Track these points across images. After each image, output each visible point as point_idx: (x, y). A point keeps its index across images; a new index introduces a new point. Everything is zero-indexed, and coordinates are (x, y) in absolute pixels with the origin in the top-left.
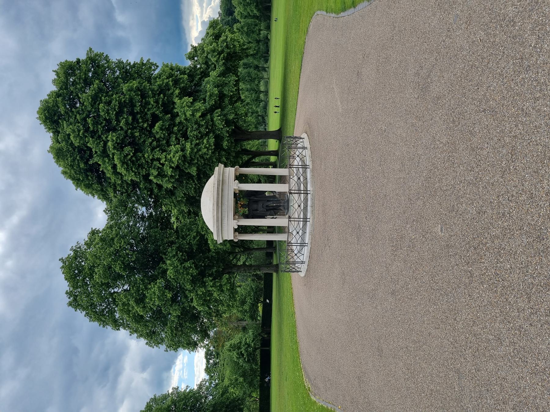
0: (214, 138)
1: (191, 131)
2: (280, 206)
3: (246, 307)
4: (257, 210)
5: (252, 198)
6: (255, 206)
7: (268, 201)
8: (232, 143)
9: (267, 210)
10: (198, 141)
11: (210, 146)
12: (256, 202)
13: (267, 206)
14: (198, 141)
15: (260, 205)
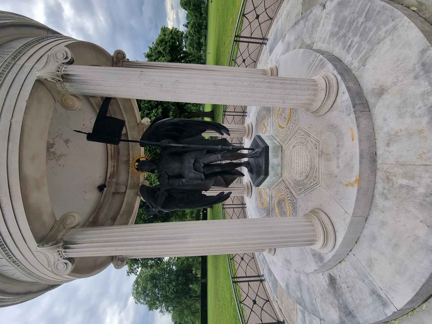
0: (162, 109)
1: (143, 104)
2: (240, 165)
3: (194, 215)
4: (180, 176)
5: (165, 142)
6: (174, 167)
7: (210, 152)
8: (176, 114)
9: (207, 176)
10: (148, 112)
11: (158, 115)
12: (179, 155)
13: (207, 165)
14: (148, 112)
15: (189, 161)
